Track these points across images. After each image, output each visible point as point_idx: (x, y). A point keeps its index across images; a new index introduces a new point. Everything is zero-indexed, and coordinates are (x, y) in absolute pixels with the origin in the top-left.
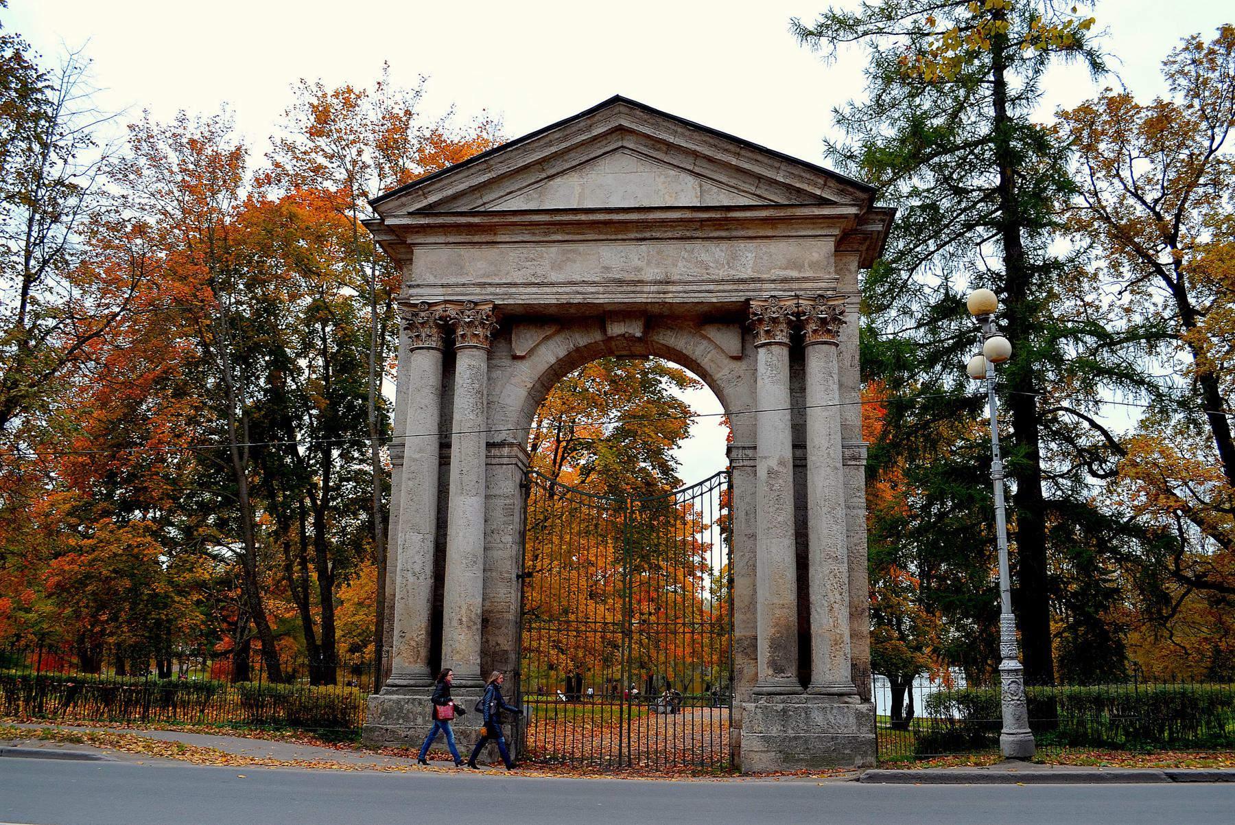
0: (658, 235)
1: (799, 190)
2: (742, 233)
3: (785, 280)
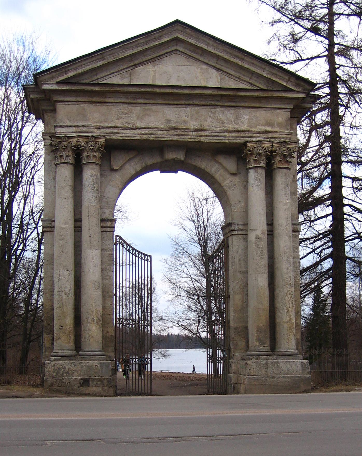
0: (197, 102)
1: (274, 82)
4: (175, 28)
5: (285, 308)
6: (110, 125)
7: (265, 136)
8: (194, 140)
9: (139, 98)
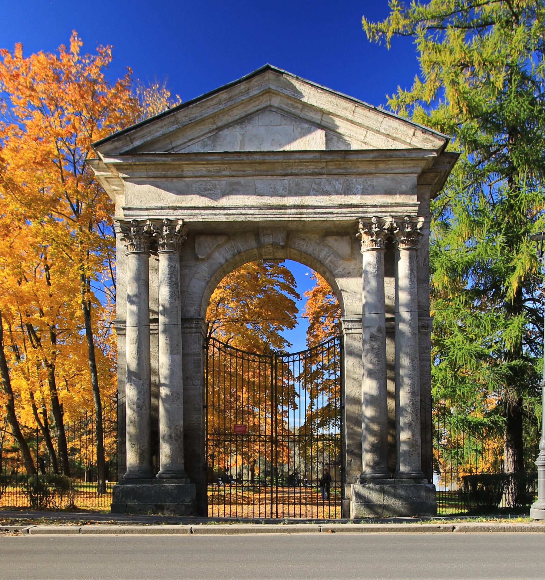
6: (189, 205)
8: (293, 219)
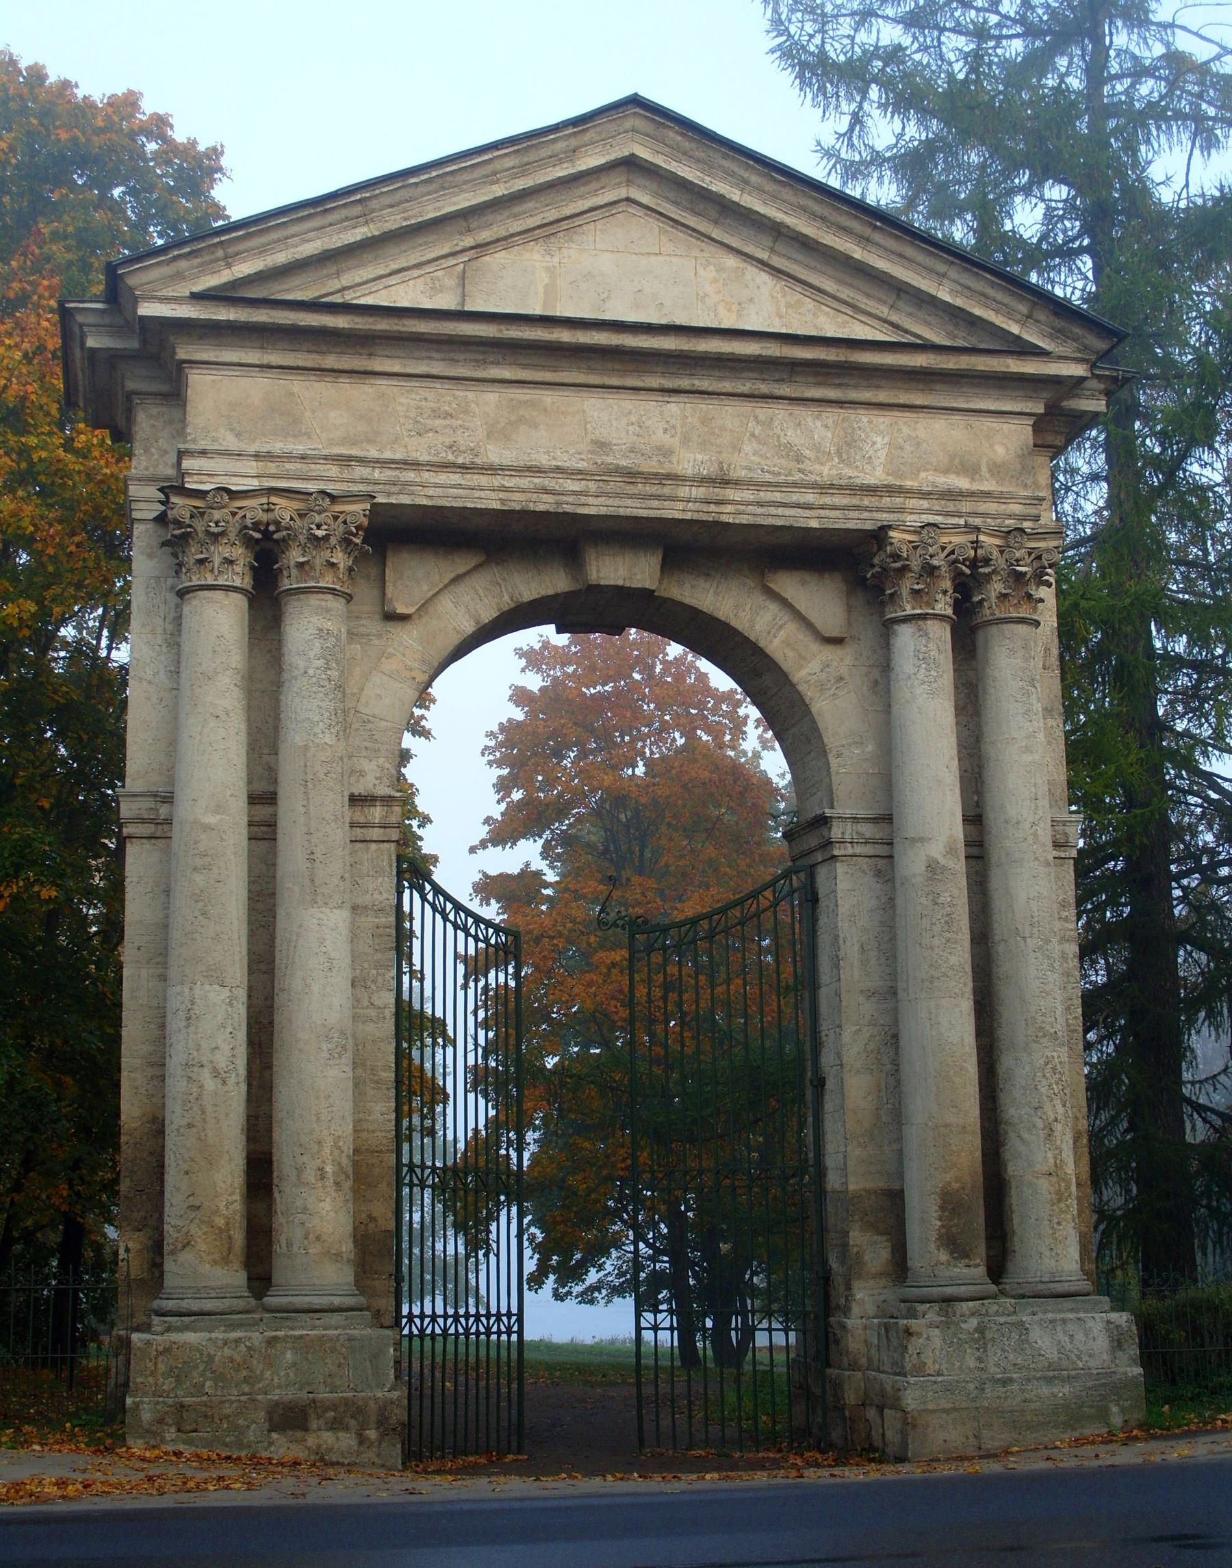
0: (705, 384)
1: (974, 322)
2: (867, 395)
3: (951, 495)
4: (628, 124)
5: (1040, 1124)
6: (388, 455)
7: (951, 506)
8: (696, 517)
9: (496, 363)
